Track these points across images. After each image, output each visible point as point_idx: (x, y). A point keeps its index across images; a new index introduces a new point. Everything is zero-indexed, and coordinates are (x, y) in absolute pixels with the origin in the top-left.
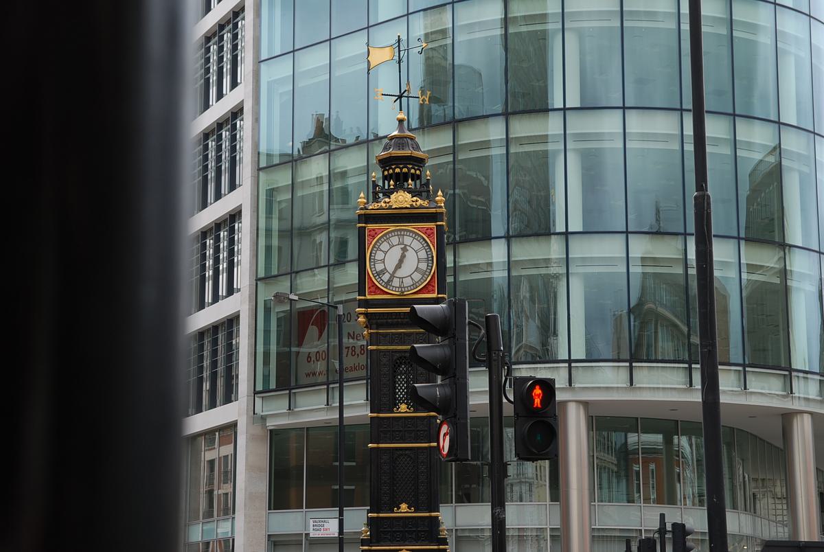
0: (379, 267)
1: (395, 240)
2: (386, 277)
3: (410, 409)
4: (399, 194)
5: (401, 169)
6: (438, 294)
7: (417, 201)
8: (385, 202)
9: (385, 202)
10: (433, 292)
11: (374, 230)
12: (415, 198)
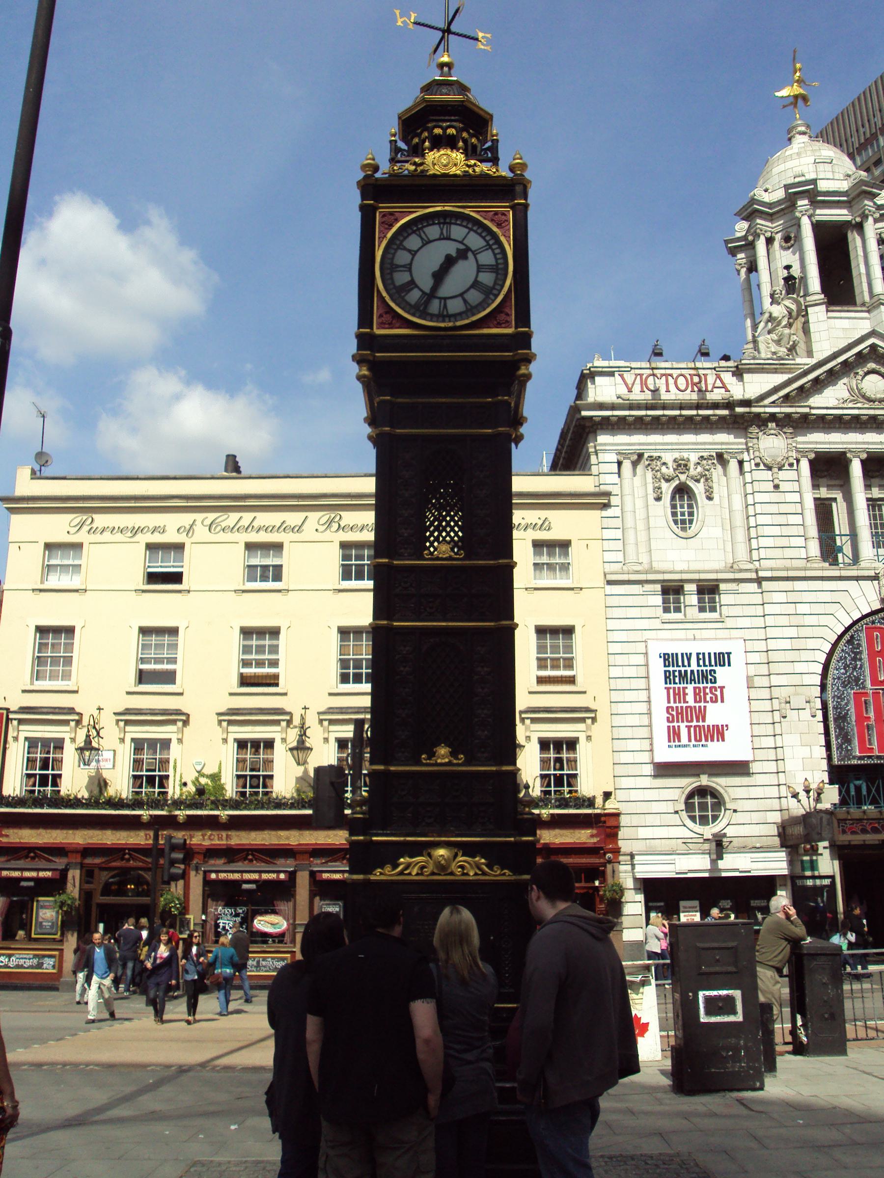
0: (401, 278)
1: (433, 231)
2: (414, 296)
3: (456, 554)
4: (442, 152)
5: (445, 129)
6: (516, 327)
7: (475, 165)
8: (415, 164)
9: (415, 164)
10: (507, 324)
11: (391, 214)
12: (473, 162)
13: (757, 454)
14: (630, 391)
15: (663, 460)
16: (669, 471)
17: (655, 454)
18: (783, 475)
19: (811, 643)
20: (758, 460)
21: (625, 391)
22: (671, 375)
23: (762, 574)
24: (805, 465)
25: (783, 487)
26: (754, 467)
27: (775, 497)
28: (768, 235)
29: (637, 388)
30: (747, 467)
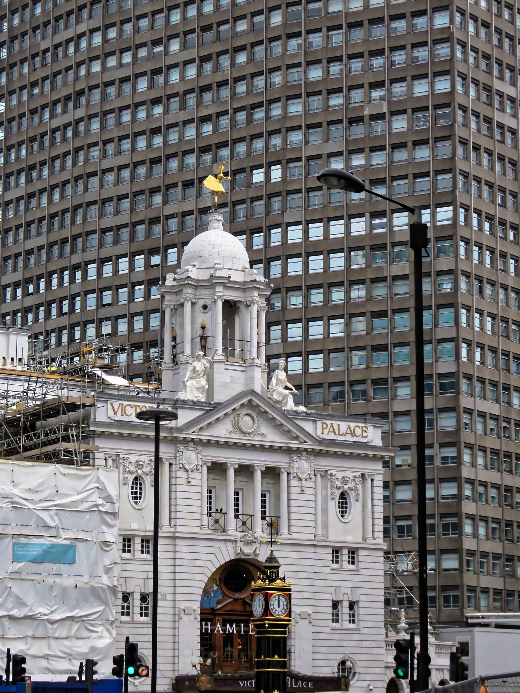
13: (181, 462)
14: (115, 414)
15: (130, 460)
16: (132, 468)
17: (126, 456)
18: (193, 475)
19: (198, 577)
20: (181, 466)
21: (111, 413)
22: (139, 406)
23: (177, 535)
24: (205, 469)
25: (193, 482)
26: (178, 469)
27: (188, 488)
28: (193, 301)
29: (119, 413)
30: (173, 466)
